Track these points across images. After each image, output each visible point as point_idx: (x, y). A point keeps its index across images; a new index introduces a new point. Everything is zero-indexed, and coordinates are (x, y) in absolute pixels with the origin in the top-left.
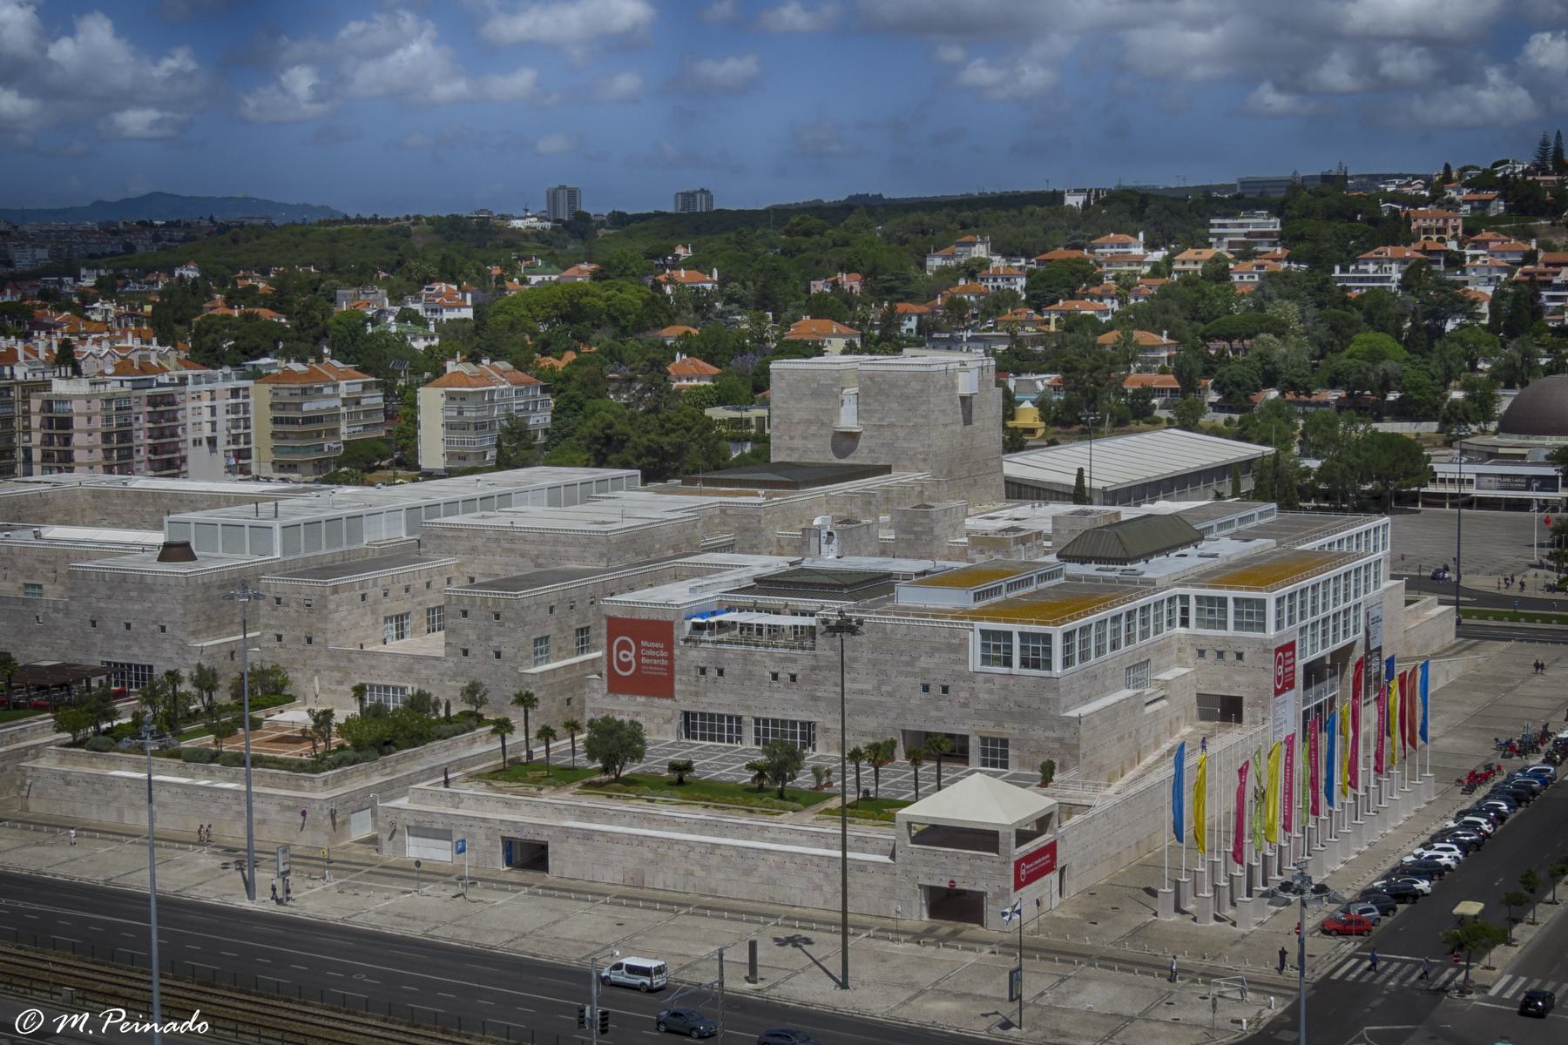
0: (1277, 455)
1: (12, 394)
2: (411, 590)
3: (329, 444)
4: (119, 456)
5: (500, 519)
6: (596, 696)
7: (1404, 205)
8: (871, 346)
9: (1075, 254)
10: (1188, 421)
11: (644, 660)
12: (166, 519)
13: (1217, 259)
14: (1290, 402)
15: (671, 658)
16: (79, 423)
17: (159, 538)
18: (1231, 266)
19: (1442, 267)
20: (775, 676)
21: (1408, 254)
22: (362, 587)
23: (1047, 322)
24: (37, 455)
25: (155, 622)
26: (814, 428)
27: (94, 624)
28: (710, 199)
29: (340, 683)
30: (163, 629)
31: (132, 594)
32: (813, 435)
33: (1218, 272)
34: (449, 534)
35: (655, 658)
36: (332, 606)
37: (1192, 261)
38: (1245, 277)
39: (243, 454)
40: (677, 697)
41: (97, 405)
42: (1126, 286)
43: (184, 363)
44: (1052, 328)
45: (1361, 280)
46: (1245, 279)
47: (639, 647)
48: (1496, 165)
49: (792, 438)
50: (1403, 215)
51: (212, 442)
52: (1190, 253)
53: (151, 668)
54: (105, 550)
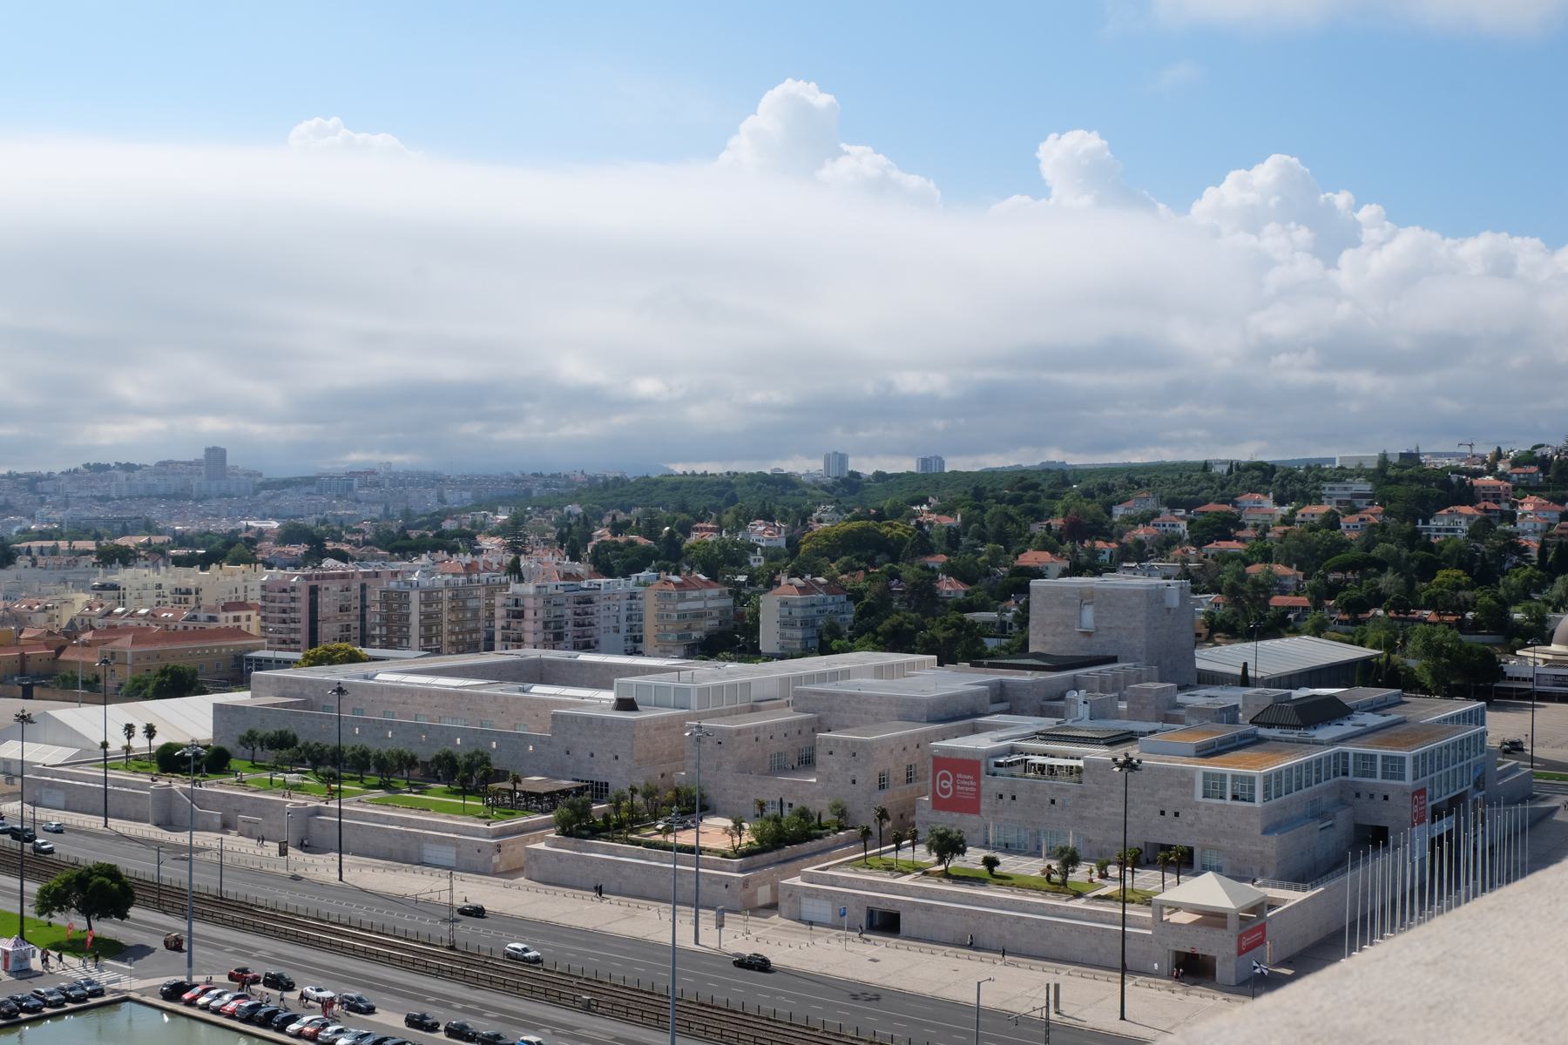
1: (450, 594)
2: (789, 735)
3: (695, 635)
4: (555, 637)
5: (842, 687)
6: (924, 812)
7: (1468, 476)
8: (1075, 570)
11: (958, 787)
12: (616, 681)
13: (1331, 512)
14: (1391, 618)
15: (978, 787)
16: (529, 614)
17: (610, 696)
20: (1053, 802)
22: (756, 732)
24: (498, 636)
25: (611, 752)
26: (1060, 629)
27: (568, 753)
28: (942, 463)
29: (741, 798)
30: (617, 758)
31: (596, 732)
32: (1061, 634)
33: (1332, 522)
34: (813, 696)
35: (966, 786)
36: (736, 745)
39: (638, 640)
40: (982, 814)
41: (540, 602)
43: (594, 574)
47: (955, 779)
49: (1045, 635)
51: (617, 631)
53: (607, 784)
54: (580, 703)
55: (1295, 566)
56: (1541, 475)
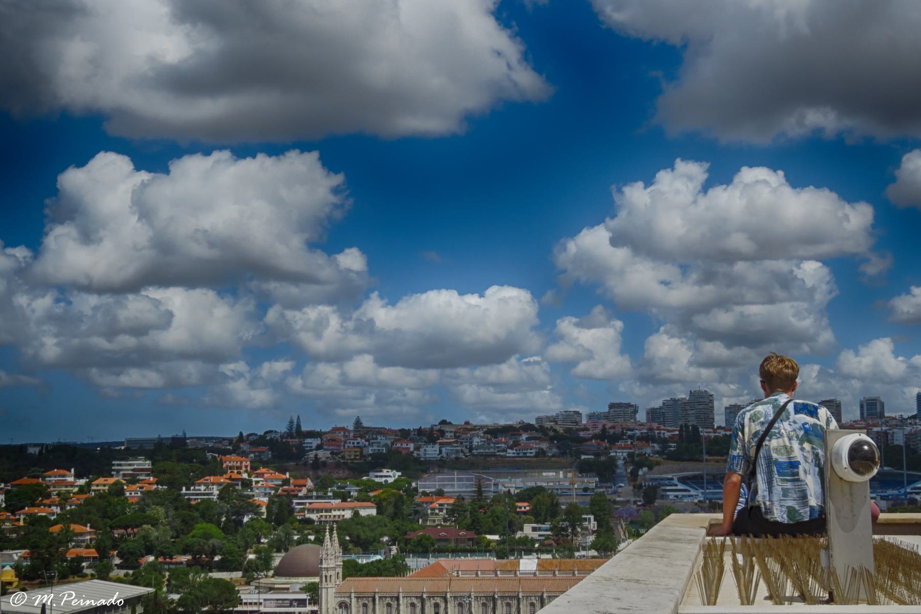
0: (156, 593)
7: (219, 454)
9: (34, 481)
10: (103, 574)
13: (117, 483)
14: (161, 563)
18: (125, 487)
19: (239, 488)
21: (222, 480)
23: (18, 520)
33: (118, 490)
37: (102, 484)
38: (132, 493)
42: (64, 498)
44: (22, 523)
45: (197, 495)
46: (133, 494)
48: (266, 433)
50: (219, 459)
52: (101, 480)
55: (89, 525)
56: (270, 453)
